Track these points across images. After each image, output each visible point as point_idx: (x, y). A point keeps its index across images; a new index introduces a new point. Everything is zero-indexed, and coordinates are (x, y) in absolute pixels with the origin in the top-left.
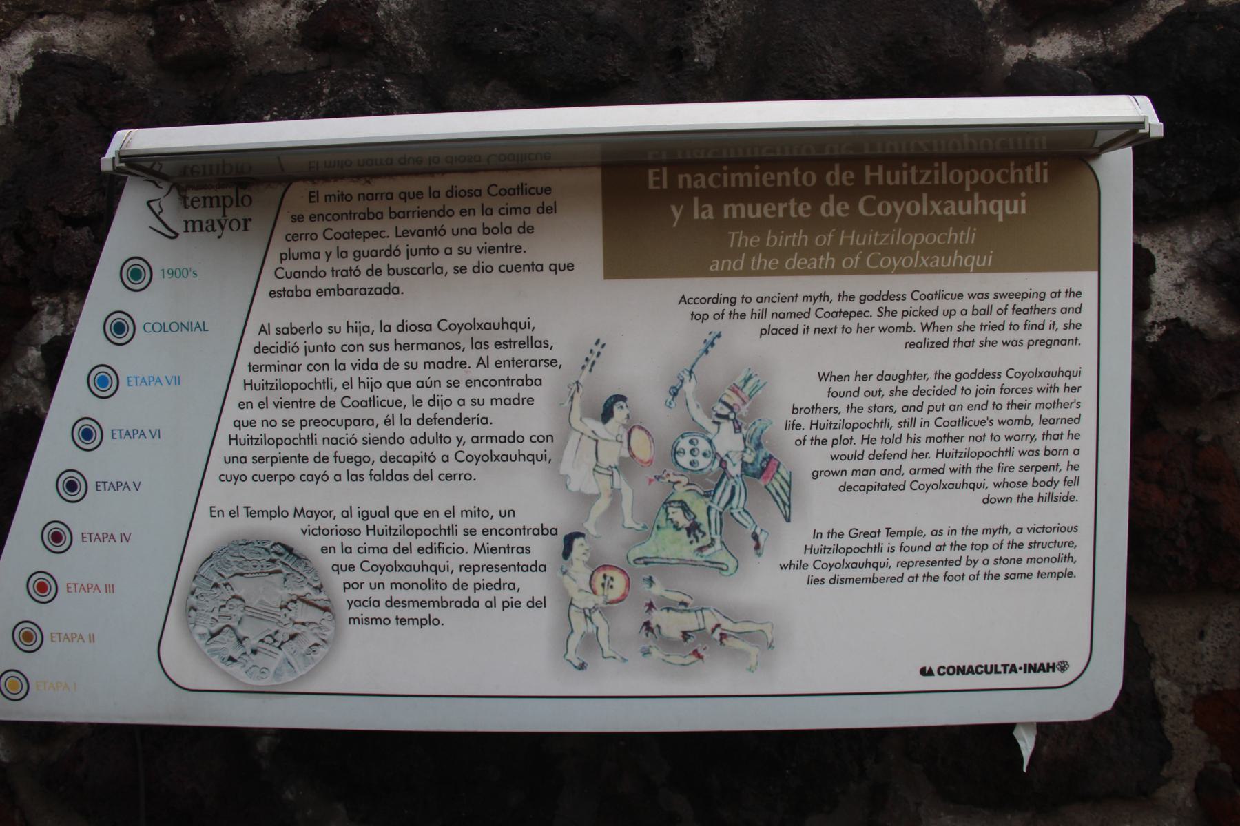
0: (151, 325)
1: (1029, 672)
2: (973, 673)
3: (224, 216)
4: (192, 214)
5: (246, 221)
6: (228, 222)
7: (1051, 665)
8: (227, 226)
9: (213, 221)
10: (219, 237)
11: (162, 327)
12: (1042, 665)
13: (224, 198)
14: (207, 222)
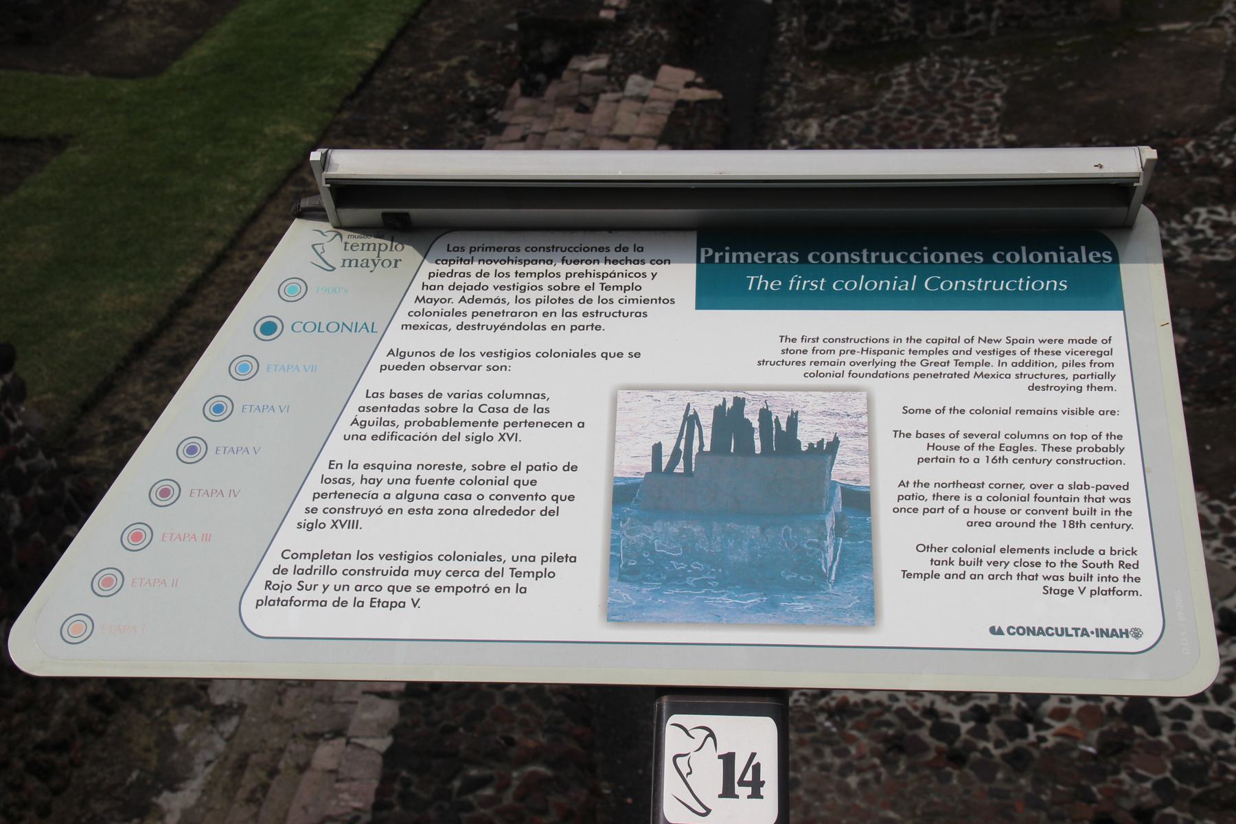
0: (303, 324)
1: (1102, 636)
2: (1044, 635)
3: (378, 257)
4: (350, 255)
5: (396, 261)
6: (381, 261)
7: (1124, 631)
8: (379, 265)
9: (368, 260)
10: (371, 271)
11: (317, 327)
12: (1114, 630)
13: (380, 245)
14: (363, 261)
